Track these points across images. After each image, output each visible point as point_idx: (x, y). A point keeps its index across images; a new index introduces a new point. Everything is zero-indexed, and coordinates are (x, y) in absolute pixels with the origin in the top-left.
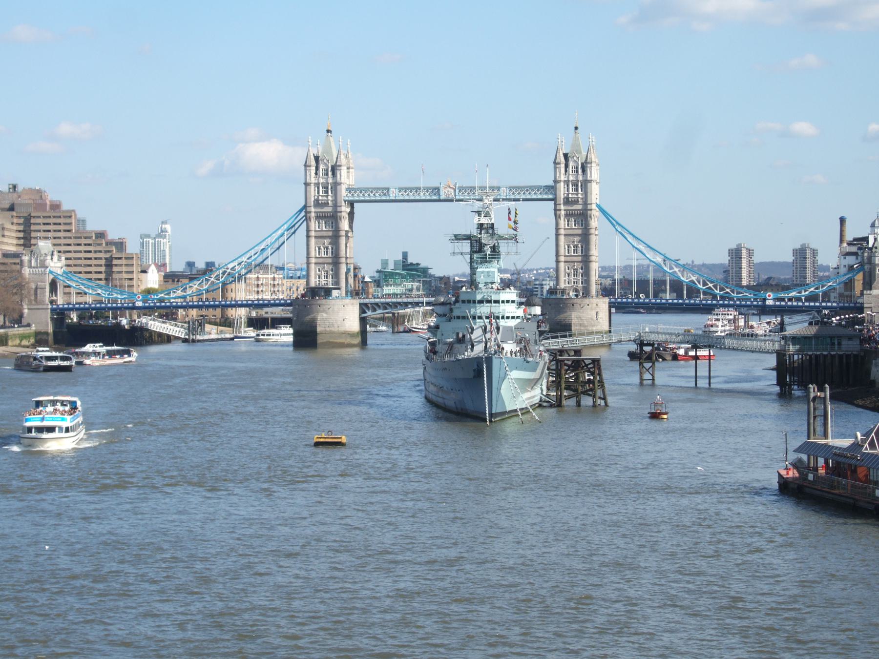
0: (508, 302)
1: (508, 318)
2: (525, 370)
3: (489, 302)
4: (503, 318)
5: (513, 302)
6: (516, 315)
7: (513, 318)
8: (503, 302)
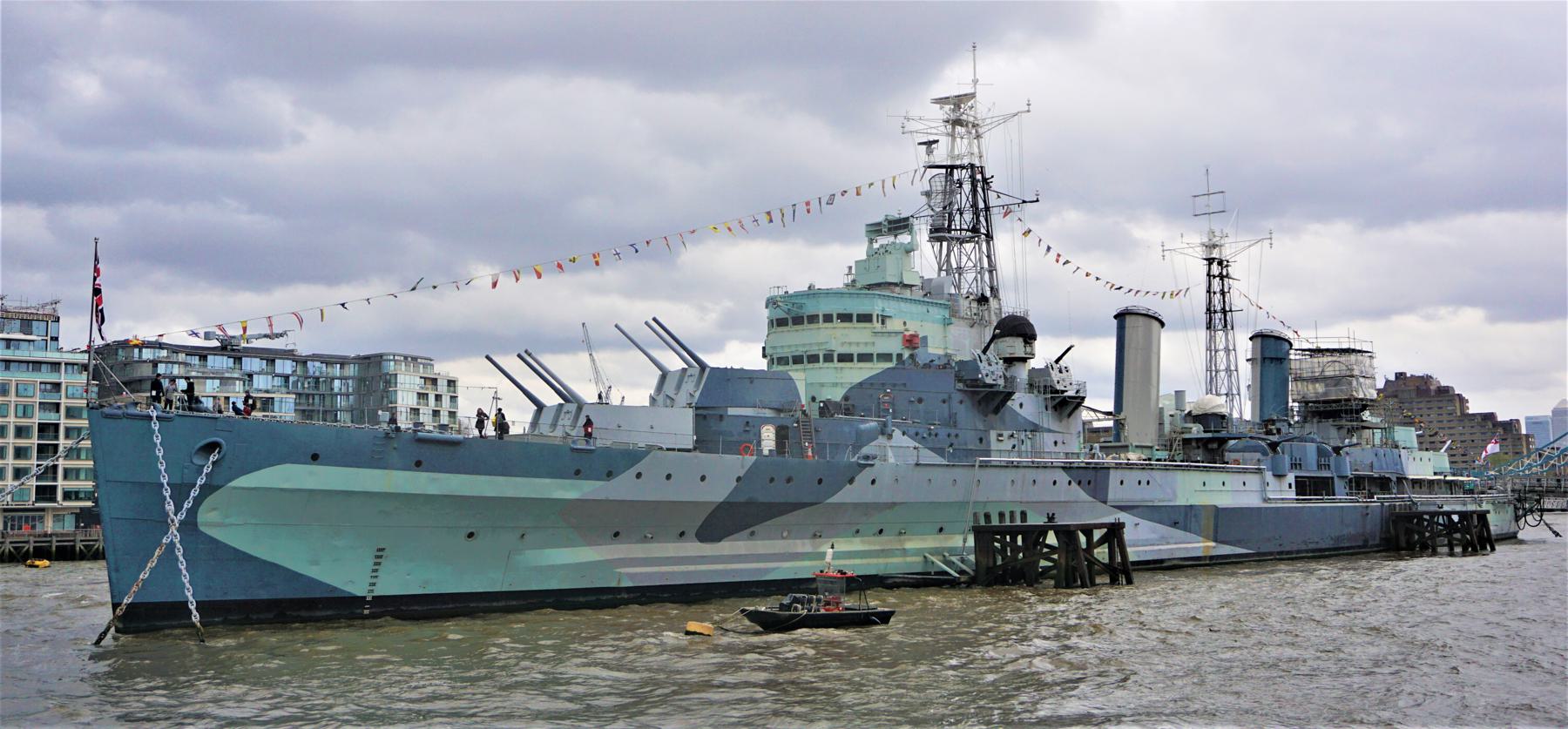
0: (845, 318)
1: (845, 358)
2: (418, 464)
3: (798, 320)
4: (828, 358)
5: (865, 318)
6: (875, 350)
7: (864, 358)
8: (828, 318)
